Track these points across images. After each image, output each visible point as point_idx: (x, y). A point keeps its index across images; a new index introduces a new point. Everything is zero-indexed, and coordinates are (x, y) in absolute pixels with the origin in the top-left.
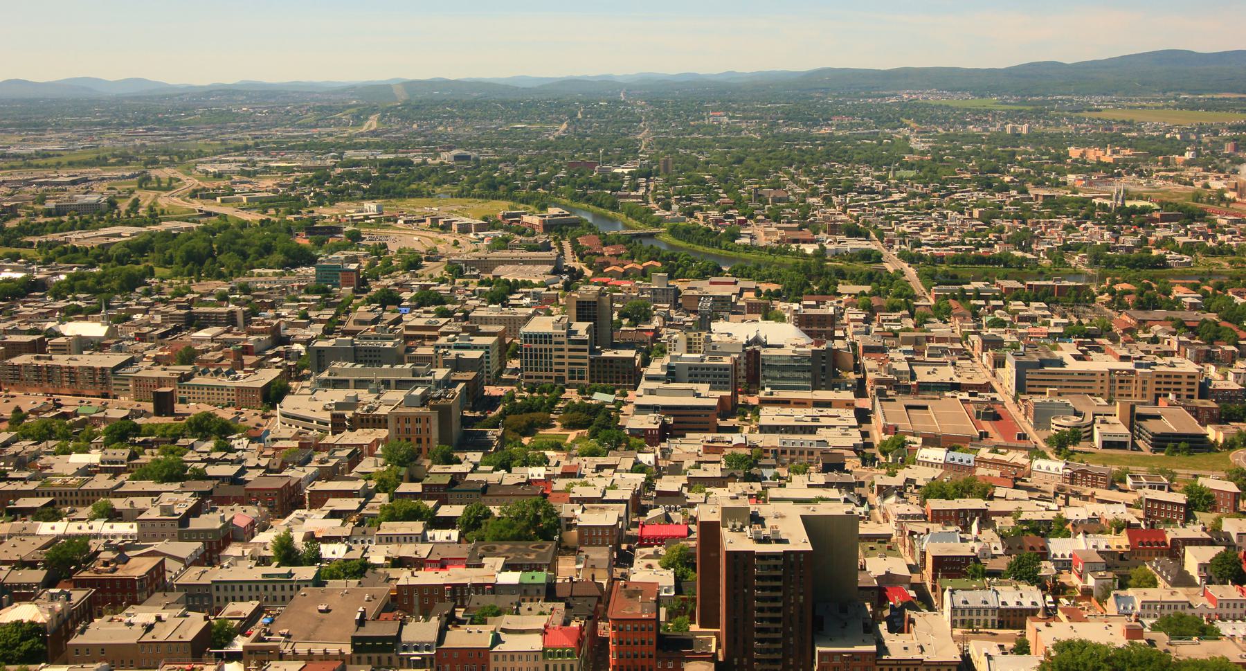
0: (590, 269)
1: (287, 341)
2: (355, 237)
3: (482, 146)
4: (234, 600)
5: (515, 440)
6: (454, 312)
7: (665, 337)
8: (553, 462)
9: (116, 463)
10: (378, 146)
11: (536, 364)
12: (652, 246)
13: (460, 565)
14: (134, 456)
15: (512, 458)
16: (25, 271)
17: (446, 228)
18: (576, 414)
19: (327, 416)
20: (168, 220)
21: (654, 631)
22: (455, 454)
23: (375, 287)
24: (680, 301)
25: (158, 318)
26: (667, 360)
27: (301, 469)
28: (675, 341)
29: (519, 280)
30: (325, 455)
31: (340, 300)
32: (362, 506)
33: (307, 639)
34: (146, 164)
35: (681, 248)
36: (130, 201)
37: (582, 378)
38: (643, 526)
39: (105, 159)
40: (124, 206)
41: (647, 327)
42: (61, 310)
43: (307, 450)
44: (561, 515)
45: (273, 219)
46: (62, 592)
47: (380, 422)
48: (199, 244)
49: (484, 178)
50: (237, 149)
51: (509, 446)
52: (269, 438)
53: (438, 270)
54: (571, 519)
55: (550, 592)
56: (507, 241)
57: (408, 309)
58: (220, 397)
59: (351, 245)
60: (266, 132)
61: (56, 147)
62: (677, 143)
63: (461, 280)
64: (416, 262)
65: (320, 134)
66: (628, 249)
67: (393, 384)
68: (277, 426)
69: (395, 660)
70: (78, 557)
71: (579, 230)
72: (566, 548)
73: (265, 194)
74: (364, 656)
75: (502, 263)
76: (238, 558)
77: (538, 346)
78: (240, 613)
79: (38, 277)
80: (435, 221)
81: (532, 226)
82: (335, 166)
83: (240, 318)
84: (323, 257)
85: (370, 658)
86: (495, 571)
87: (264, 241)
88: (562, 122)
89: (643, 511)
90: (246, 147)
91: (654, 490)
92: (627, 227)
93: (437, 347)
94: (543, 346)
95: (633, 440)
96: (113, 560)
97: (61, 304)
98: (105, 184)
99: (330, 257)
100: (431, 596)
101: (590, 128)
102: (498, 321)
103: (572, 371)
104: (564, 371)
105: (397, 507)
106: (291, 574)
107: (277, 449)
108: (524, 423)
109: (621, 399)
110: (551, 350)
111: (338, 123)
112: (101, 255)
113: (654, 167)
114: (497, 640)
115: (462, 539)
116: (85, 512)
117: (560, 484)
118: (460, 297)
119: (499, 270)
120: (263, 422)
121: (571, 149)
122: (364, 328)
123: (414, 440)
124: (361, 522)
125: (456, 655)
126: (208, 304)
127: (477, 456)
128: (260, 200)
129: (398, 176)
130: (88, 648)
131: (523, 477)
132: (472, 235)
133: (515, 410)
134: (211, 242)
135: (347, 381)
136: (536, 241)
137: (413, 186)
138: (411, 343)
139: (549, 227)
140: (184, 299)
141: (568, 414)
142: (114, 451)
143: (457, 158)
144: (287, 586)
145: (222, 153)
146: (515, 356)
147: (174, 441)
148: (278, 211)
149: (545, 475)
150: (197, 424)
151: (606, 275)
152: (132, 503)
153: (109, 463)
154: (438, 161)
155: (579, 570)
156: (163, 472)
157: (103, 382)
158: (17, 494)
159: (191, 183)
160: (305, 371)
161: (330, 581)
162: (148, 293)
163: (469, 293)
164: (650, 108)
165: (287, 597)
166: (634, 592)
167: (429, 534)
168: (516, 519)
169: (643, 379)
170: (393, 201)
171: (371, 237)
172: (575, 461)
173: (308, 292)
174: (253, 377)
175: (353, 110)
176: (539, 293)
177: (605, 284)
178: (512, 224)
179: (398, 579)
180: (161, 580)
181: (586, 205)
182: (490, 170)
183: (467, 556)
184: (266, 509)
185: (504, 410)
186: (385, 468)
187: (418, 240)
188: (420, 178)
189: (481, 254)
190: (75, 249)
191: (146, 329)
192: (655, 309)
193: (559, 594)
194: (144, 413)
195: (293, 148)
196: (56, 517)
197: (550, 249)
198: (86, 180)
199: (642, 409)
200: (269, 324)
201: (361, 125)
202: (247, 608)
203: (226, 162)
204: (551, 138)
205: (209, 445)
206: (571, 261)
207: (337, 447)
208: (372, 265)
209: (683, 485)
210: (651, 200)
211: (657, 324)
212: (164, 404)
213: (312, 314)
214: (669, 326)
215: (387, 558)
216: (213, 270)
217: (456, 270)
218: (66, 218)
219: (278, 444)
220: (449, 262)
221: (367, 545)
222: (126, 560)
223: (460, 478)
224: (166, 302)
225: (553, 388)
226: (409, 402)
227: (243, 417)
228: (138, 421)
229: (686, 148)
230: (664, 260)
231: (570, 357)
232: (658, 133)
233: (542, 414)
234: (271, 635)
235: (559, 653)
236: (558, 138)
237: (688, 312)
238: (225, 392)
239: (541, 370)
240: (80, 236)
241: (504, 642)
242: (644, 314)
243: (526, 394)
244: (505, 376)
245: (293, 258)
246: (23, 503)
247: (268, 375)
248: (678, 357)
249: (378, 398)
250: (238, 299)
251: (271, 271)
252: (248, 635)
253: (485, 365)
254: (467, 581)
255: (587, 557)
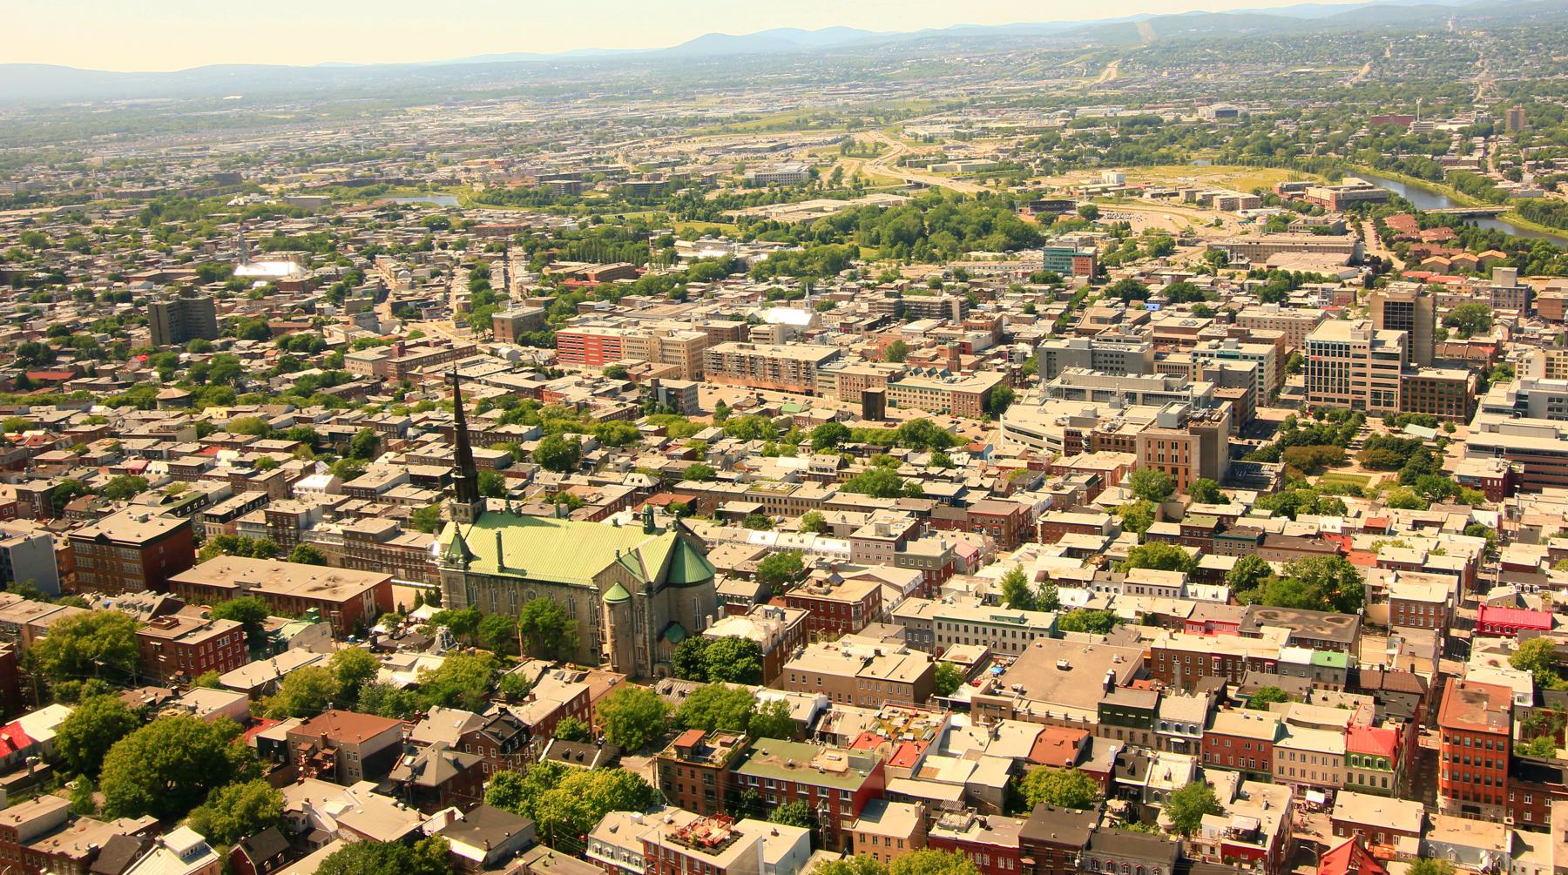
0: (1402, 259)
1: (1008, 339)
2: (1091, 214)
3: (1252, 97)
4: (958, 641)
5: (1297, 478)
6: (1216, 311)
7: (1512, 354)
8: (1352, 511)
9: (826, 470)
10: (1117, 100)
11: (1326, 383)
12: (1492, 230)
13: (1229, 632)
14: (844, 464)
15: (1297, 502)
16: (726, 249)
17: (1205, 203)
18: (1381, 451)
19: (1059, 433)
20: (873, 192)
21: (1506, 752)
22: (1222, 492)
23: (1116, 277)
24: (1534, 306)
25: (865, 307)
26: (1515, 386)
27: (1032, 494)
28: (1529, 361)
29: (1303, 272)
30: (1059, 480)
31: (1073, 292)
32: (1106, 545)
33: (1045, 699)
34: (850, 127)
35: (1537, 233)
36: (833, 170)
37: (1389, 404)
38: (1484, 608)
39: (806, 121)
40: (826, 175)
41: (1483, 340)
42: (764, 293)
43: (1037, 473)
44: (1365, 582)
45: (992, 191)
46: (776, 610)
47: (1125, 445)
48: (909, 221)
49: (1255, 139)
50: (950, 108)
51: (1290, 486)
52: (992, 454)
53: (1197, 256)
54: (1380, 588)
55: (1352, 681)
56: (1286, 221)
57: (1157, 306)
58: (934, 402)
59: (1086, 224)
60: (983, 86)
61: (754, 110)
62: (1531, 87)
63: (1226, 271)
64: (1168, 246)
65: (1047, 88)
66: (1457, 234)
67: (1139, 397)
68: (998, 438)
69: (1152, 740)
70: (790, 573)
71: (1385, 207)
72: (1372, 625)
73: (983, 162)
74: (1113, 729)
75: (1280, 249)
76: (961, 593)
77: (1330, 359)
78: (965, 658)
79: (739, 255)
80: (1190, 196)
81: (1321, 203)
82: (1065, 126)
83: (956, 310)
84: (1054, 239)
85: (1120, 733)
86: (1273, 643)
87: (982, 218)
88: (1362, 63)
89: (1483, 587)
90: (961, 106)
91: (1498, 560)
92: (1457, 204)
93: (1196, 355)
94: (1337, 360)
95: (1466, 492)
96: (827, 581)
97: (763, 287)
98: (806, 151)
99: (1061, 238)
100: (1194, 667)
101: (1403, 70)
102: (1276, 324)
103: (1376, 395)
104: (1364, 393)
105: (1150, 551)
106: (1023, 620)
107: (1002, 468)
108: (1310, 458)
109: (1446, 435)
110: (1347, 365)
111: (1070, 73)
112: (802, 233)
113: (1497, 122)
114: (1282, 732)
115: (1233, 599)
116: (795, 522)
117: (1363, 542)
118: (1224, 293)
119: (1275, 259)
120: (982, 434)
121: (1376, 100)
122: (1103, 327)
123: (1168, 470)
124: (1105, 566)
125: (1228, 744)
126: (919, 292)
127: (1249, 496)
128: (978, 169)
129: (1142, 138)
130: (805, 676)
131: (1312, 528)
132: (1239, 213)
133: (1299, 440)
134: (922, 218)
135: (1083, 391)
136: (1326, 222)
137: (1163, 151)
138: (1161, 349)
139: (1344, 203)
140: (893, 286)
141: (1370, 451)
142: (824, 457)
143: (1219, 114)
144: (1019, 633)
145: (932, 113)
146: (1296, 371)
147: (886, 451)
148: (998, 182)
149: (1343, 528)
150: (911, 433)
151: (1424, 268)
152: (844, 518)
153: (818, 469)
154: (1195, 118)
155: (1392, 656)
156: (876, 485)
157: (807, 377)
158: (726, 497)
159: (898, 148)
160: (1031, 377)
161: (1069, 633)
162: (853, 278)
163: (1235, 287)
164: (1491, 41)
165: (1019, 647)
166: (1475, 697)
167: (1191, 588)
168: (1305, 580)
169: (1479, 410)
170: (1138, 169)
171: (1110, 214)
172: (1383, 513)
173: (1034, 280)
174: (971, 381)
175: (1088, 56)
176: (1329, 290)
177: (1423, 280)
178: (1294, 200)
179: (1152, 640)
180: (877, 609)
181: (1396, 174)
182: (1264, 129)
183: (1240, 621)
184: (990, 539)
185: (1283, 440)
186: (1133, 502)
187: (1167, 219)
188: (1172, 140)
189: (1253, 237)
190: (776, 226)
191: (852, 319)
192: (1496, 317)
193: (1364, 684)
194: (850, 416)
195: (1015, 105)
196: (766, 525)
197: (1345, 232)
198: (786, 147)
199: (1477, 449)
200: (990, 318)
201: (1098, 75)
202: (974, 653)
203: (938, 123)
204: (1347, 85)
205: (926, 458)
206: (1374, 248)
207: (1073, 472)
208: (1112, 249)
209: (1543, 558)
210: (1491, 167)
211: (1500, 337)
212: (873, 406)
213: (1040, 308)
214: (1518, 340)
215: (1138, 613)
216: (925, 252)
217: (1219, 258)
218: (765, 190)
219: (1004, 463)
220: (1210, 248)
221: (1112, 594)
222: (841, 582)
223: (1228, 521)
224: (873, 288)
225: (1349, 415)
226: (1162, 422)
227: (959, 427)
228: (848, 424)
229: (1546, 94)
230: (1511, 249)
231: (1373, 376)
232: (1502, 75)
233: (1333, 447)
234: (1002, 688)
235: (1367, 761)
236: (1357, 85)
237: (1547, 322)
238: (940, 397)
239: (1333, 391)
240: (780, 210)
241: (1291, 736)
242: (1481, 323)
243: (1311, 420)
244: (1283, 396)
245: (1016, 239)
246: (732, 506)
247: (987, 380)
248: (1532, 383)
249: (1122, 414)
250: (954, 287)
251: (990, 255)
252: (977, 685)
253: (1258, 380)
254: (1244, 654)
255: (1403, 640)
